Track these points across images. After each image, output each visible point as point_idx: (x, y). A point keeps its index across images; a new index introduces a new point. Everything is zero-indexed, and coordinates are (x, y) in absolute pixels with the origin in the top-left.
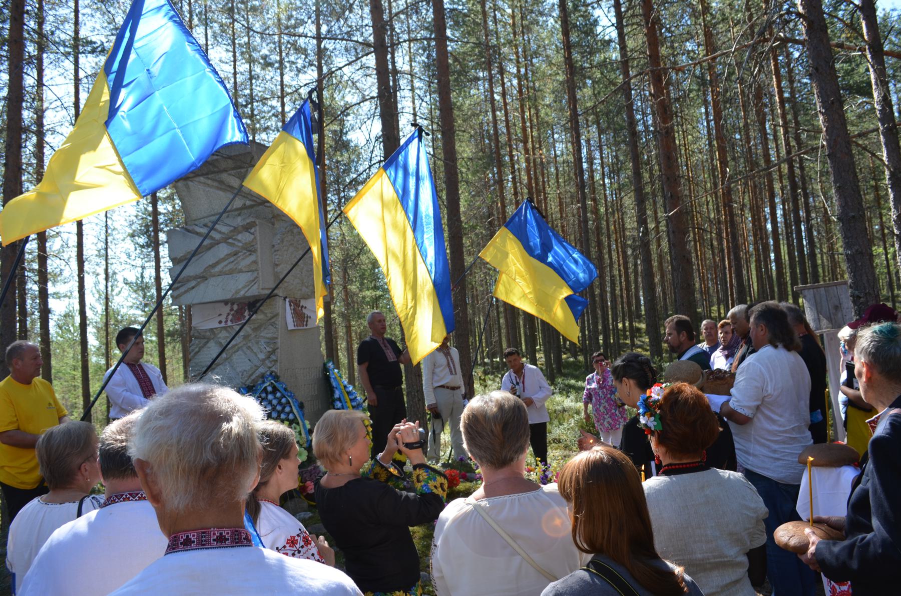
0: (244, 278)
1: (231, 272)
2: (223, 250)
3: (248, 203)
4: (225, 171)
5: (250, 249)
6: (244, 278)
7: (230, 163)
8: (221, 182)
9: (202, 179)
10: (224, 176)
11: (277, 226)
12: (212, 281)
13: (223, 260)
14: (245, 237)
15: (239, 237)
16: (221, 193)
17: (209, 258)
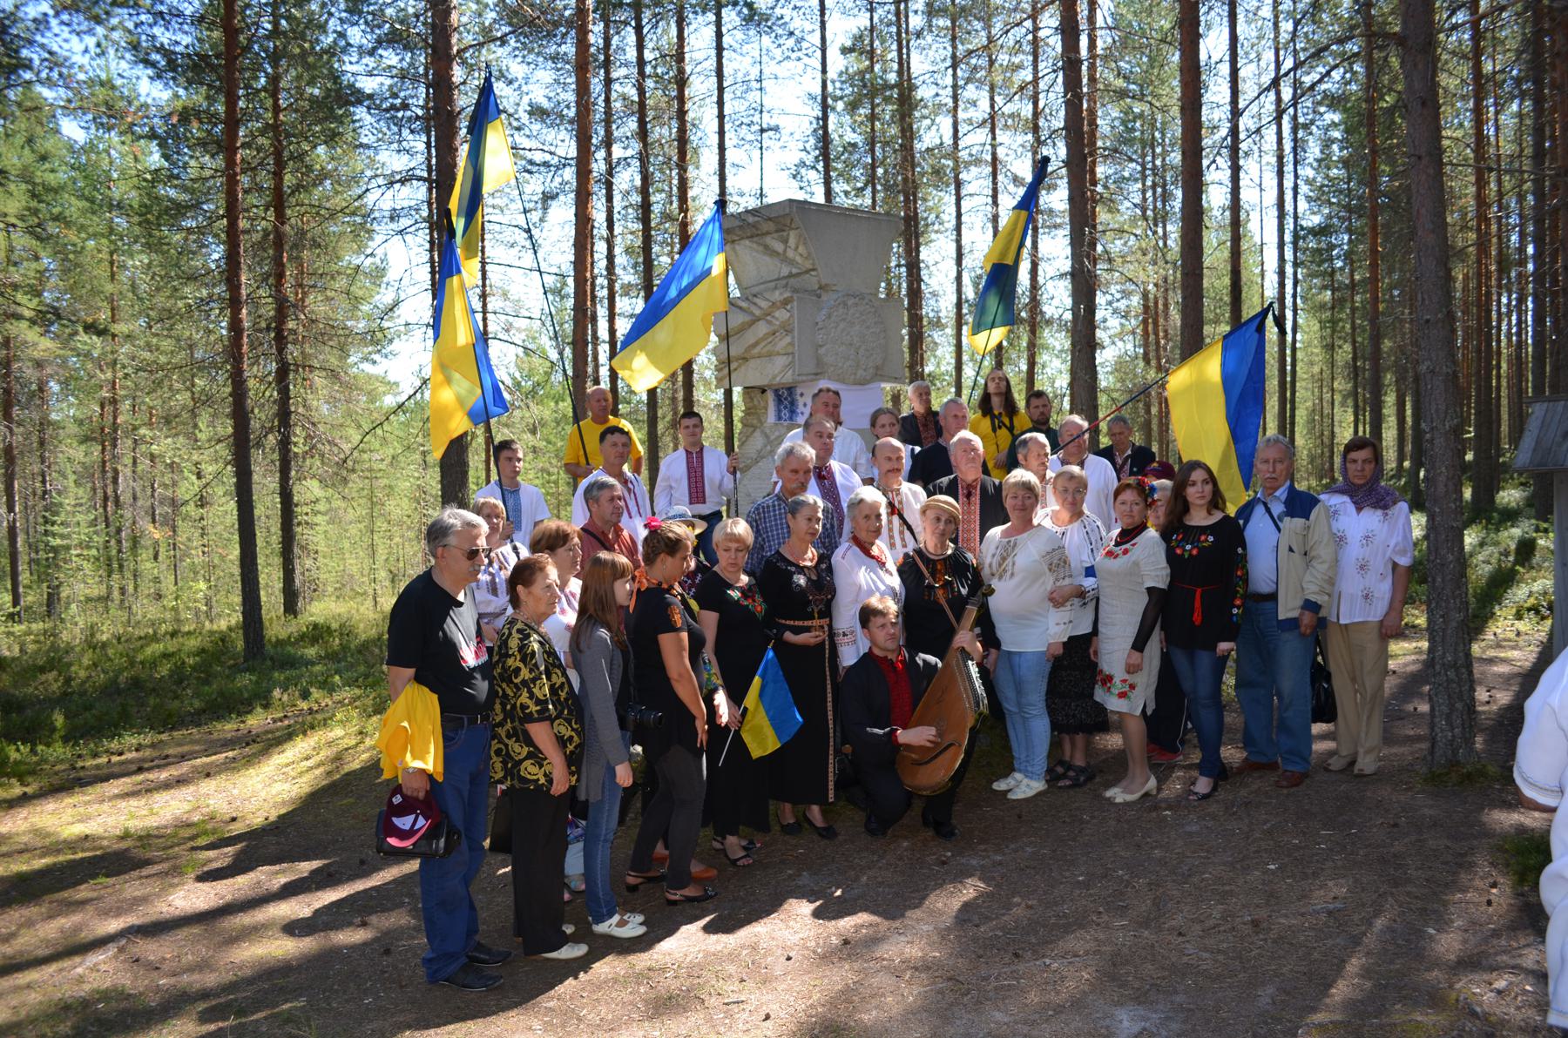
0: (781, 361)
1: (770, 355)
2: (762, 329)
3: (794, 271)
4: (768, 233)
5: (787, 329)
6: (781, 361)
7: (770, 226)
8: (766, 247)
9: (747, 242)
10: (769, 240)
11: (824, 297)
12: (752, 363)
13: (763, 339)
14: (782, 315)
15: (777, 314)
16: (767, 258)
17: (750, 337)
